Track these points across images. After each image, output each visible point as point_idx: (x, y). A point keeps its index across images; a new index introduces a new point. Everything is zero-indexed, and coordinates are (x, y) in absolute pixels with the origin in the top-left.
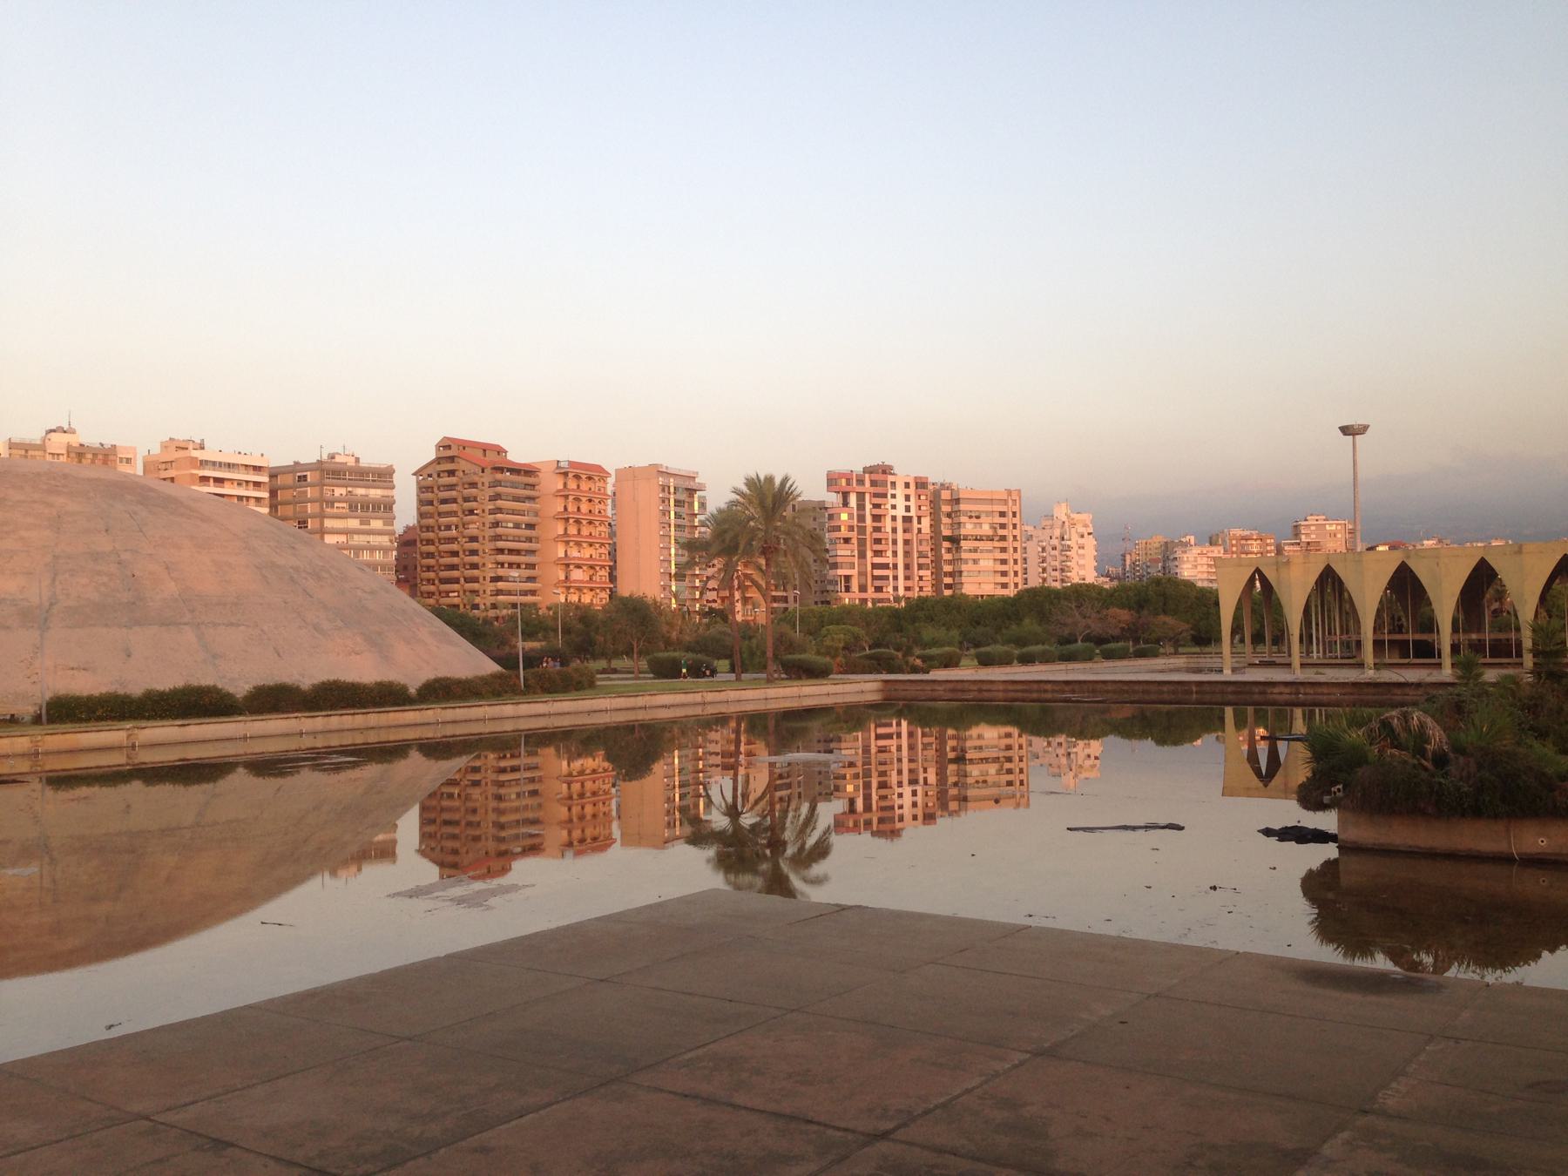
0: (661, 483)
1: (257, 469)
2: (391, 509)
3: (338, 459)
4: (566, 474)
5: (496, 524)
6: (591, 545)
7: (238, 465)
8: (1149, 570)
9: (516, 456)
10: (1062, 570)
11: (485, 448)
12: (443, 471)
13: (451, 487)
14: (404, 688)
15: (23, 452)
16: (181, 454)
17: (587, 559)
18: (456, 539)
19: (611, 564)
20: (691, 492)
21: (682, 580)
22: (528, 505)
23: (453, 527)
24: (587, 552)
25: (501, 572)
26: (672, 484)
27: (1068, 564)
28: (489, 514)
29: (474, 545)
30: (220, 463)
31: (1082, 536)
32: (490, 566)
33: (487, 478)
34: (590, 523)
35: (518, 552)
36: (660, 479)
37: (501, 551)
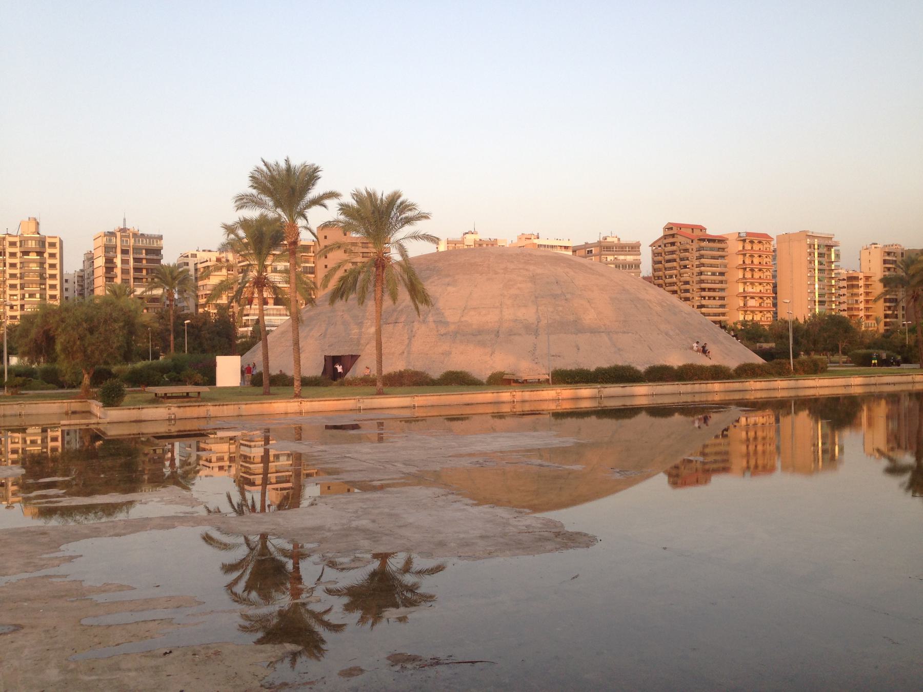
0: (808, 243)
1: (566, 248)
2: (639, 266)
3: (609, 240)
4: (744, 241)
5: (701, 273)
6: (760, 284)
7: (557, 246)
9: (712, 231)
11: (693, 228)
12: (668, 243)
13: (673, 252)
14: (728, 369)
15: (454, 245)
16: (528, 242)
17: (758, 293)
18: (676, 283)
19: (774, 295)
20: (829, 247)
21: (823, 305)
22: (721, 261)
23: (674, 276)
24: (758, 288)
25: (704, 302)
26: (816, 243)
28: (696, 267)
29: (687, 287)
30: (548, 246)
32: (697, 299)
33: (695, 245)
34: (760, 270)
35: (714, 290)
36: (808, 240)
37: (704, 290)
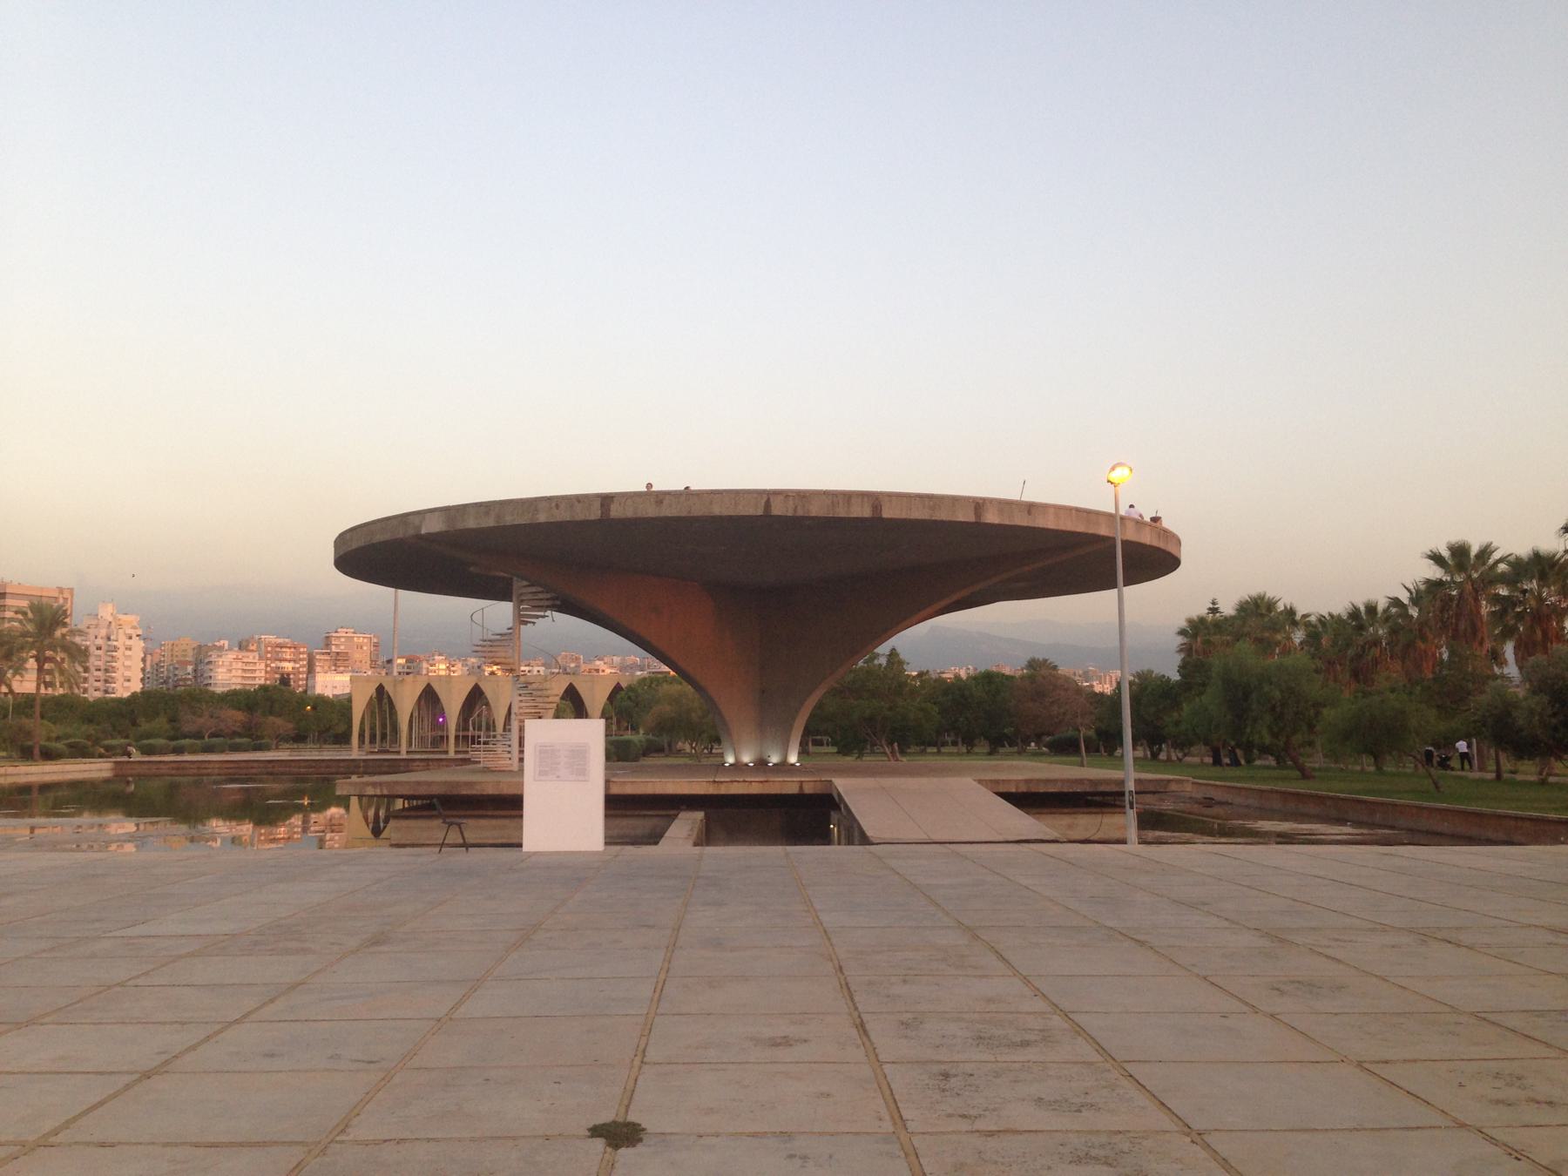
8: (177, 672)
10: (106, 671)
27: (114, 664)
31: (130, 638)
